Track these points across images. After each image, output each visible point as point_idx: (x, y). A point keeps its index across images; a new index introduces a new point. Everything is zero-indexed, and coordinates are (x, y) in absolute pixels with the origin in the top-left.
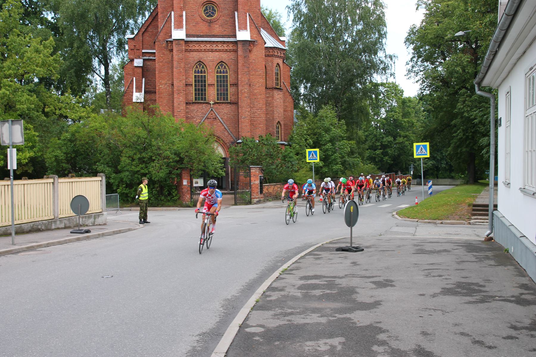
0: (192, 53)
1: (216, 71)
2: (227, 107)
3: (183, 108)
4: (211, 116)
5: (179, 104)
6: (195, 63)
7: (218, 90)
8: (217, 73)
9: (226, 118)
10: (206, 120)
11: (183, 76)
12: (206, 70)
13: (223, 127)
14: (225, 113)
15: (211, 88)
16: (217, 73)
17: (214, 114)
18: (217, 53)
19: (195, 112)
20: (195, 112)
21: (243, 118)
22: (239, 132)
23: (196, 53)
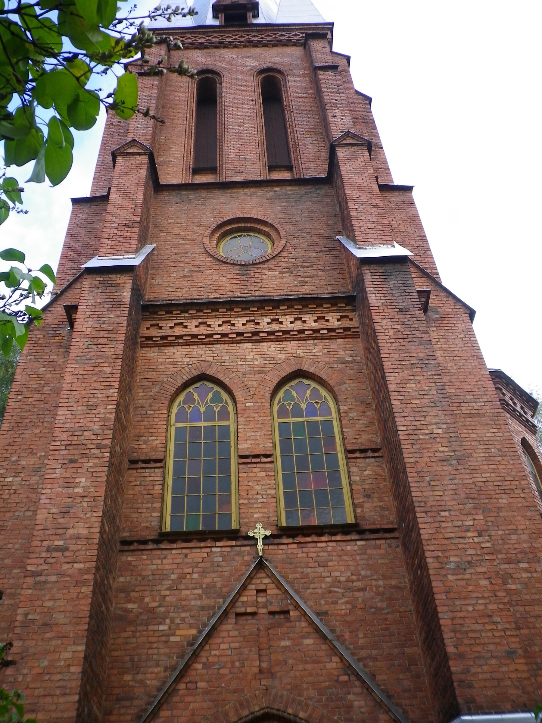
0: (169, 351)
1: (276, 408)
2: (346, 553)
3: (83, 531)
4: (256, 604)
5: (64, 514)
6: (180, 382)
7: (288, 481)
8: (283, 412)
9: (342, 607)
10: (229, 626)
11: (110, 387)
12: (231, 408)
13: (334, 664)
14: (336, 582)
15: (257, 468)
16: (283, 412)
17: (272, 591)
18: (276, 347)
19: (167, 583)
20: (167, 583)
21: (459, 569)
22: (446, 657)
23: (186, 350)
